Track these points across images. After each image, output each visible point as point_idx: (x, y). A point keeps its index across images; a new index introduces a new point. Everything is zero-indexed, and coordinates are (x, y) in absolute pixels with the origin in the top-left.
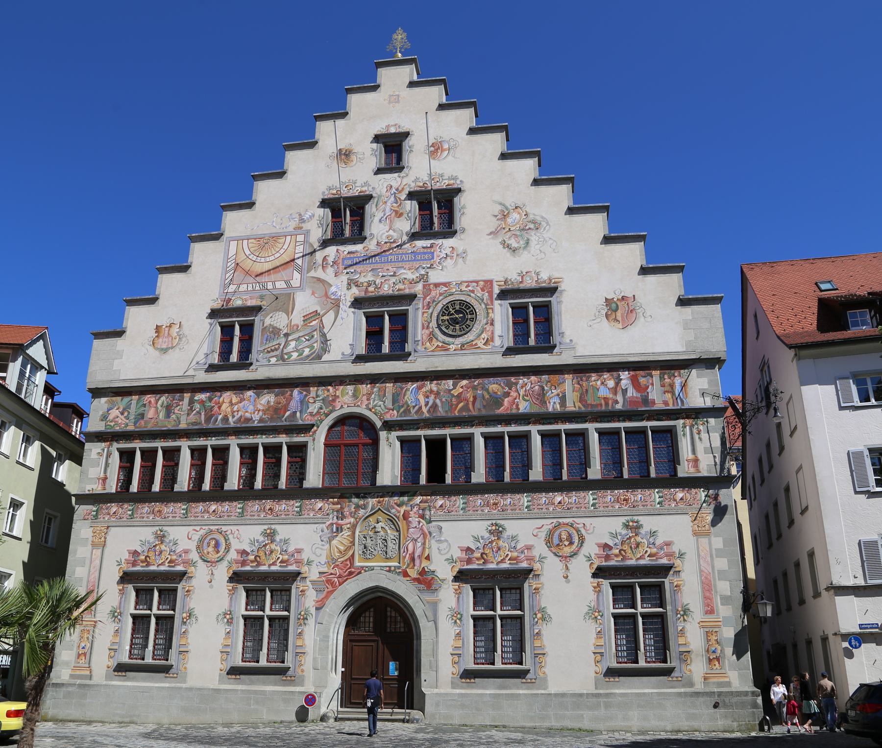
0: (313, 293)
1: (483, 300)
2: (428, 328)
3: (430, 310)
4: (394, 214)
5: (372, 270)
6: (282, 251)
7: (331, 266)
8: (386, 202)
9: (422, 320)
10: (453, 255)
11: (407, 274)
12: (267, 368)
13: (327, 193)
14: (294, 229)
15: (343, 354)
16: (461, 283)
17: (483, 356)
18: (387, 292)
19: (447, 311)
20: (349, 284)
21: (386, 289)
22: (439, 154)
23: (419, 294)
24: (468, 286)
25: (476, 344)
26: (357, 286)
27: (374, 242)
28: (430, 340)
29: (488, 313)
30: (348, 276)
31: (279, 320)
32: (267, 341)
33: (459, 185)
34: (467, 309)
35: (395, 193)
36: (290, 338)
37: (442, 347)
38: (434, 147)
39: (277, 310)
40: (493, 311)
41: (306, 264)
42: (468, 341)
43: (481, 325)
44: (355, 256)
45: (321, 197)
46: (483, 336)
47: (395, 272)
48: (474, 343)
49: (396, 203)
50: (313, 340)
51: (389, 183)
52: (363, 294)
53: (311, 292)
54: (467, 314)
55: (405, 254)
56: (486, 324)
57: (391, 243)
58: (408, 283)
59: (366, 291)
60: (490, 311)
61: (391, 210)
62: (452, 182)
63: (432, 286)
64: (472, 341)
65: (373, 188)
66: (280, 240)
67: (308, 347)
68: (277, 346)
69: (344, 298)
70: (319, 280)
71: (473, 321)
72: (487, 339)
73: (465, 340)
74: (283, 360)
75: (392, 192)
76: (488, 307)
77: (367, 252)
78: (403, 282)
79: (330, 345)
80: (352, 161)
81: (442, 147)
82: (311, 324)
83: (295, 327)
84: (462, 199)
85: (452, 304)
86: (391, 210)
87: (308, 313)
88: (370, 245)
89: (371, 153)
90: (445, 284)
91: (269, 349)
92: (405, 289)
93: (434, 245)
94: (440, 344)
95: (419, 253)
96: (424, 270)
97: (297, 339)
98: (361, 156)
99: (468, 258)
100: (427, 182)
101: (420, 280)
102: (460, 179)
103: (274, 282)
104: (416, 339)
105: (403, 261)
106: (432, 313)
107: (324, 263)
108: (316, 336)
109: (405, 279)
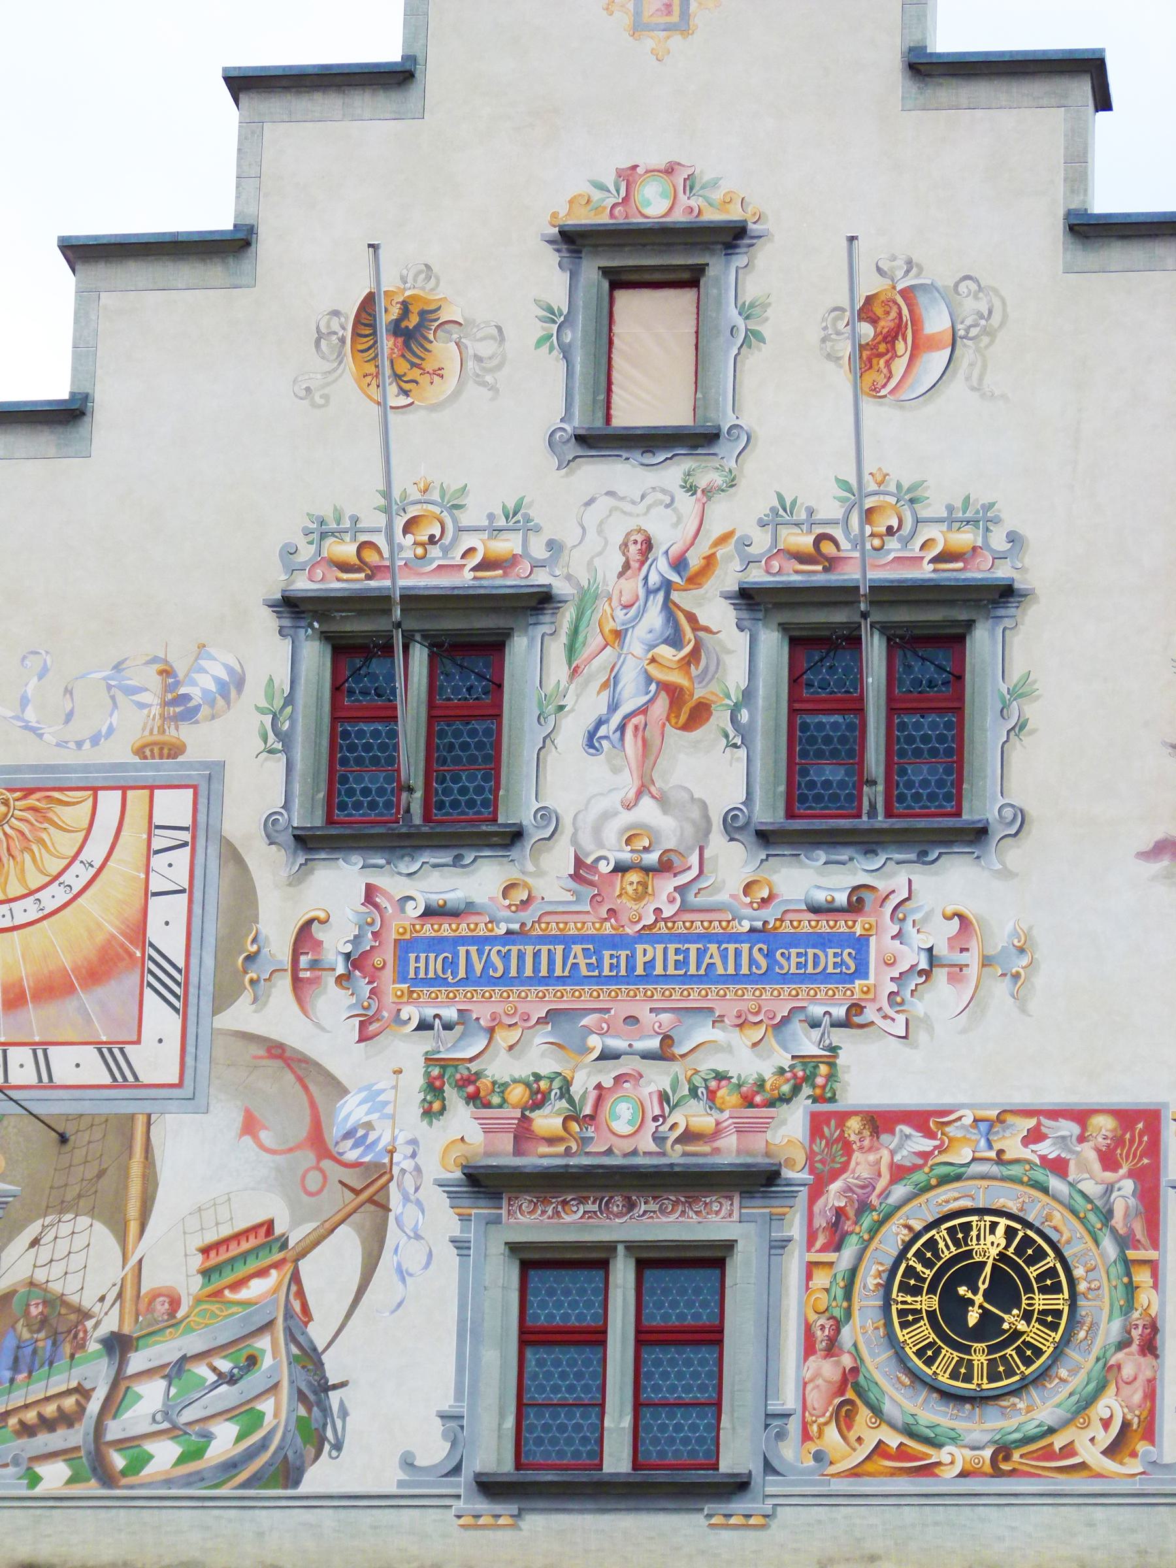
0: (250, 1126)
1: (1108, 1215)
2: (832, 1348)
3: (845, 1256)
4: (661, 706)
5: (552, 1016)
6: (77, 876)
7: (340, 980)
8: (619, 635)
9: (802, 1305)
10: (963, 958)
11: (729, 1049)
12: (20, 1517)
13: (306, 553)
14: (140, 752)
15: (408, 1463)
16: (1000, 1119)
17: (1099, 1514)
18: (627, 1145)
19: (928, 1264)
20: (434, 1088)
21: (622, 1126)
22: (899, 366)
23: (790, 1163)
24: (1034, 1136)
25: (1069, 1450)
26: (474, 1099)
27: (560, 860)
28: (844, 1416)
29: (1131, 1289)
30: (425, 1043)
31: (77, 1261)
32: (15, 1367)
33: (999, 557)
34: (1031, 1261)
35: (668, 586)
36: (137, 1362)
37: (902, 1453)
38: (874, 321)
39: (63, 1207)
40: (1155, 1275)
41: (209, 962)
42: (1031, 1429)
43: (1096, 1351)
44: (463, 930)
45: (275, 582)
46: (1101, 1409)
47: (667, 1040)
48: (1059, 1441)
49: (675, 641)
50: (254, 1382)
51: (632, 524)
52: (503, 1153)
53: (238, 1119)
54: (1029, 1289)
55: (719, 939)
56: (1123, 1345)
57: (647, 870)
58: (734, 1099)
59: (523, 1133)
60: (1142, 1277)
61: (649, 679)
62: (964, 538)
63: (854, 1124)
64: (1051, 1431)
65: (552, 545)
66: (59, 809)
67: (227, 1414)
68: (69, 1403)
69: (408, 1165)
70: (277, 1051)
71: (1054, 1327)
72: (1126, 1425)
73: (1010, 1424)
74: (107, 1477)
75: (654, 579)
76: (1132, 1254)
77: (529, 916)
78: (712, 1095)
79: (344, 1413)
80: (439, 373)
81: (916, 321)
82: (244, 1294)
83: (162, 1307)
84: (1017, 641)
85: (952, 1231)
86: (649, 679)
87: (226, 1231)
88: (540, 873)
89: (538, 330)
90: (921, 1120)
91: (31, 1416)
92: (717, 1133)
93: (868, 897)
94: (893, 1440)
95: (794, 940)
96: (816, 1034)
97: (176, 1370)
98: (486, 349)
99: (1040, 981)
100: (837, 533)
101: (796, 1089)
102: (1011, 522)
103: (41, 1048)
104: (774, 1406)
105: (708, 976)
106: (853, 1272)
107: (304, 960)
108: (267, 1362)
109: (721, 1077)
